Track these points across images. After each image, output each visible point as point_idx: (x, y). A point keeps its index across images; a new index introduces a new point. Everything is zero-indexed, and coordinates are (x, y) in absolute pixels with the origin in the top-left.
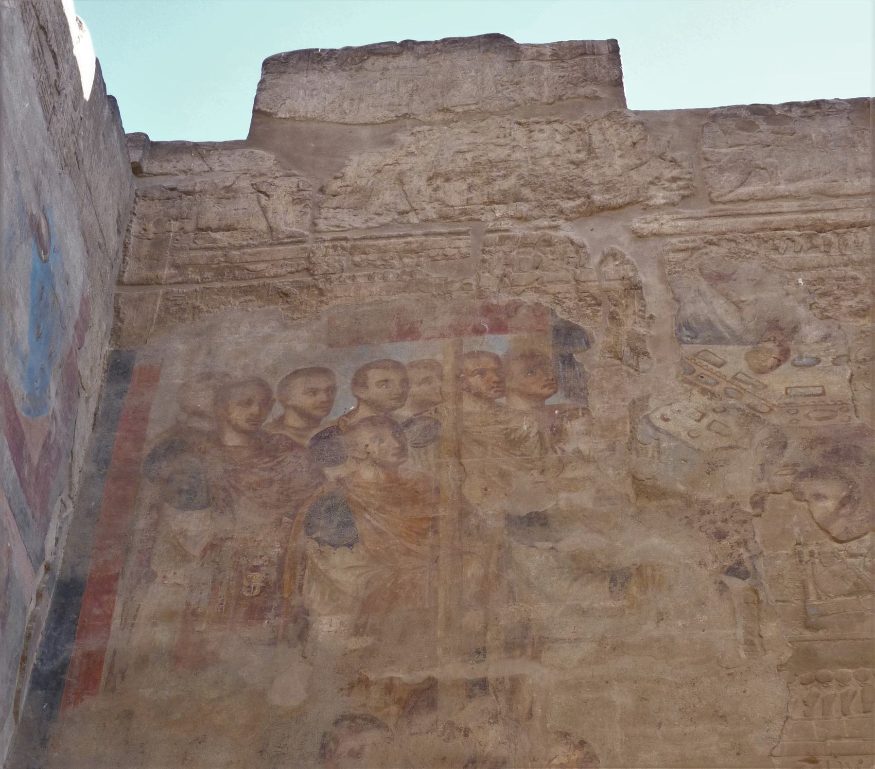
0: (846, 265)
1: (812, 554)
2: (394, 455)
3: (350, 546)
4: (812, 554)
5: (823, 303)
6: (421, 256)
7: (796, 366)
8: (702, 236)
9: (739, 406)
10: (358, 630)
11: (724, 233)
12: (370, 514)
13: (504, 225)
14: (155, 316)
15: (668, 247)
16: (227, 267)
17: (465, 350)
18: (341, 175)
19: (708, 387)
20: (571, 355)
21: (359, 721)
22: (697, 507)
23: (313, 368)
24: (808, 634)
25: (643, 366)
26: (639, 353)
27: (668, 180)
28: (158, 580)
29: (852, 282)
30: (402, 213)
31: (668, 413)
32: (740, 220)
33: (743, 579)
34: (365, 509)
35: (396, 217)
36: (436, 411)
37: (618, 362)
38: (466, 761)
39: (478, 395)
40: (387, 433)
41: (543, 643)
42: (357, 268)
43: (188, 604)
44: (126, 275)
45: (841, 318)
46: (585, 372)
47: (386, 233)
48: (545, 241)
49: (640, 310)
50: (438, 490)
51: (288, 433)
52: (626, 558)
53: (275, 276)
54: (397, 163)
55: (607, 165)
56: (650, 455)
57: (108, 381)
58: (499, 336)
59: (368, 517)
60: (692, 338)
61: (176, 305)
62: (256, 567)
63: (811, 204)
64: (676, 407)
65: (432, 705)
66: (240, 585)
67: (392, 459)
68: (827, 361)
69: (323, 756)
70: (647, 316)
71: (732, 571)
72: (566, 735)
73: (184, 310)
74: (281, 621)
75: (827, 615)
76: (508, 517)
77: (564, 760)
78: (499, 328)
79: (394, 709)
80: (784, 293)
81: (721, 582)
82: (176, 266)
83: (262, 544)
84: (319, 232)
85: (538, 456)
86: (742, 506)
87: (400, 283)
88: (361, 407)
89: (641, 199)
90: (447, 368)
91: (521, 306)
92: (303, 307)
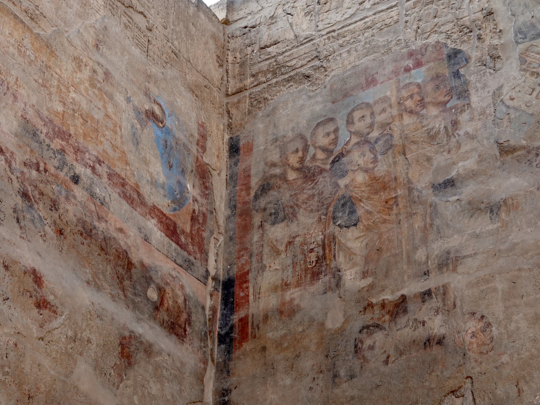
2: (371, 163)
3: (355, 225)
6: (373, 30)
10: (364, 275)
12: (363, 203)
16: (278, 68)
17: (402, 85)
19: (535, 70)
20: (458, 70)
21: (371, 328)
22: (534, 152)
25: (498, 66)
28: (267, 269)
31: (514, 95)
34: (360, 200)
36: (390, 129)
37: (484, 67)
38: (425, 341)
39: (411, 112)
41: (458, 260)
42: (342, 48)
43: (283, 280)
44: (230, 90)
46: (466, 80)
49: (494, 28)
50: (396, 179)
52: (499, 196)
56: (505, 126)
57: (230, 157)
58: (418, 70)
59: (362, 205)
60: (523, 39)
62: (312, 249)
64: (517, 89)
66: (305, 262)
69: (356, 352)
70: (498, 31)
72: (473, 314)
73: (260, 102)
74: (327, 278)
77: (474, 329)
78: (419, 64)
79: (387, 317)
82: (253, 76)
83: (313, 235)
85: (446, 142)
88: (352, 137)
92: (317, 82)
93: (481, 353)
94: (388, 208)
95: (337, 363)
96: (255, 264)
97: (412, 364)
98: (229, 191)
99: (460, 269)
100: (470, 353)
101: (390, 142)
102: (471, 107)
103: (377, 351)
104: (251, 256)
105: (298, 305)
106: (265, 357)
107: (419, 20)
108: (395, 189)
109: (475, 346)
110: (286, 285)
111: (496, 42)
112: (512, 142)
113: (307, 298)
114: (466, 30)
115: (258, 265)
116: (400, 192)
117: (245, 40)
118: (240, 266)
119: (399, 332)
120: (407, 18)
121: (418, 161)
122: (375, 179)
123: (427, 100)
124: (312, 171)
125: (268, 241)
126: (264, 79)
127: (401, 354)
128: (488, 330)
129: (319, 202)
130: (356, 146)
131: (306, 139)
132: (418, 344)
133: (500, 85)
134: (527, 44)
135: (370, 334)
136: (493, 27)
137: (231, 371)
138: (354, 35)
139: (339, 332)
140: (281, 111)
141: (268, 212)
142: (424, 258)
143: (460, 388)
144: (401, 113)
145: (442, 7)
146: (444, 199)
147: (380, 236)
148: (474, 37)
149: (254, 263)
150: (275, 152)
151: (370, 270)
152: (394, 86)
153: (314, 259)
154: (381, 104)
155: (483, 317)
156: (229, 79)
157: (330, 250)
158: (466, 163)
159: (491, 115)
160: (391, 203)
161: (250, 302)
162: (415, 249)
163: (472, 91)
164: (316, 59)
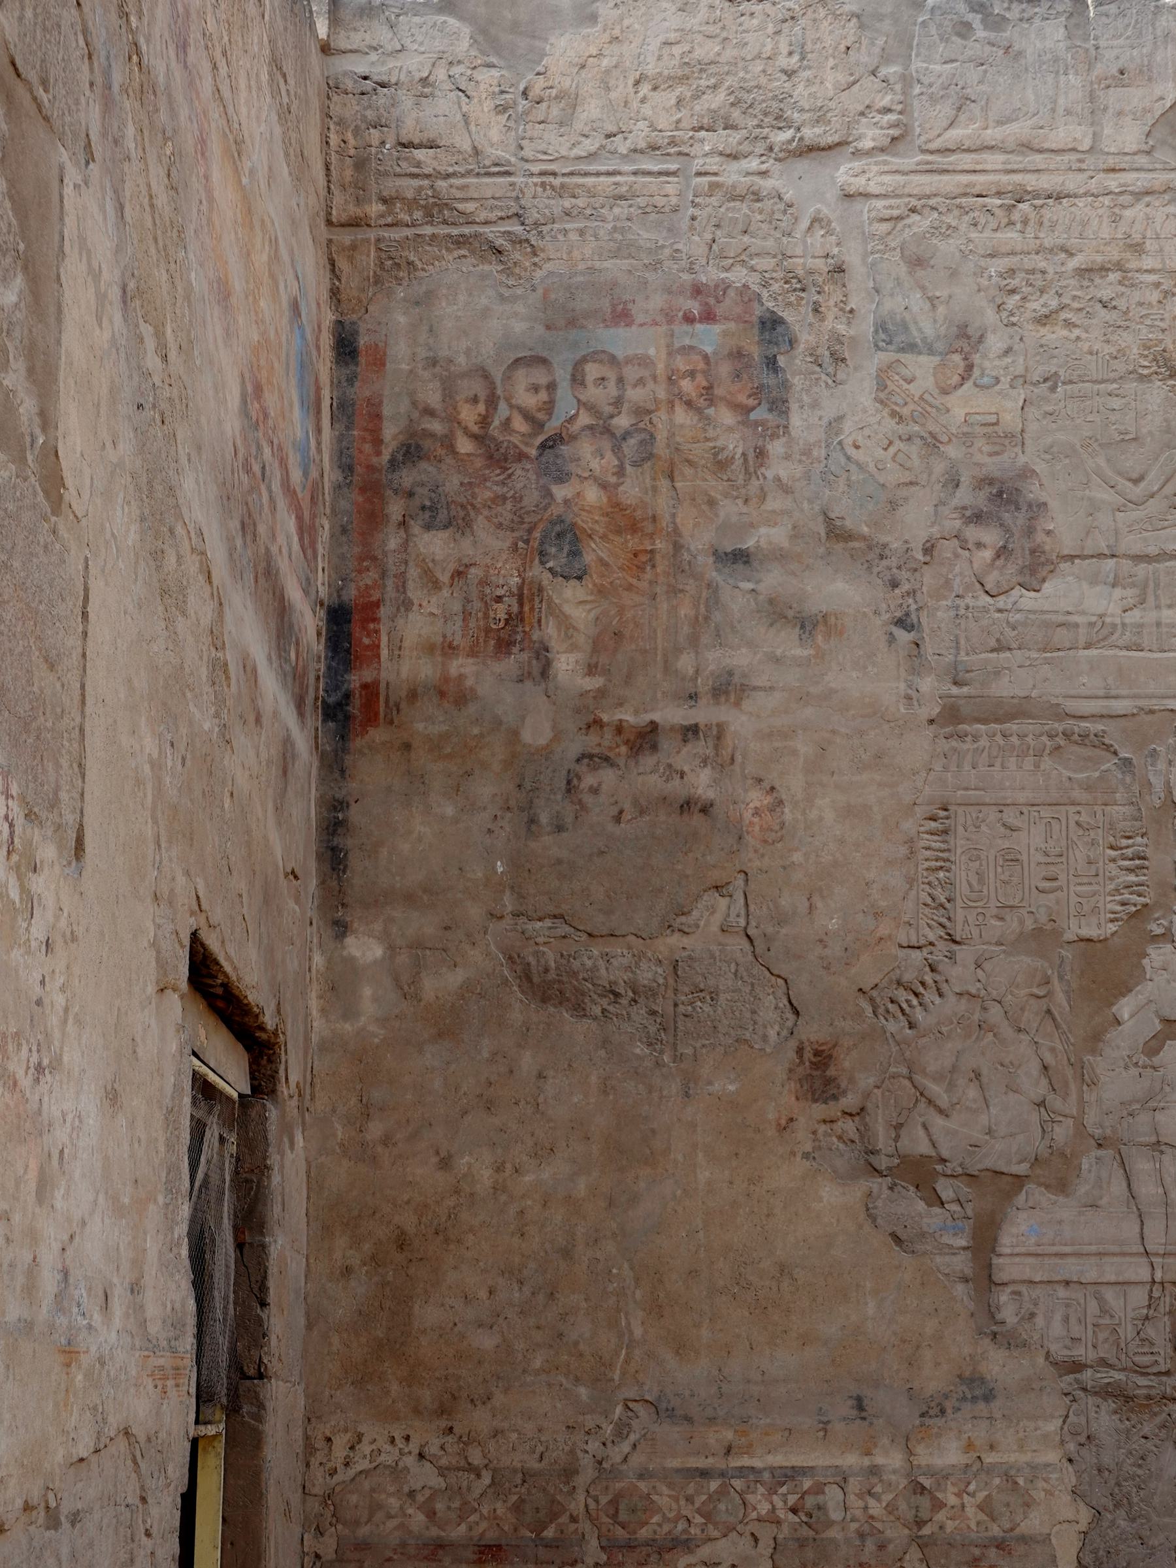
1: (967, 608)
3: (579, 578)
4: (967, 608)
10: (591, 670)
11: (929, 197)
13: (713, 163)
15: (873, 214)
16: (435, 204)
17: (677, 345)
22: (878, 551)
24: (955, 690)
25: (841, 376)
27: (879, 112)
28: (415, 608)
29: (1039, 276)
30: (608, 136)
32: (946, 178)
37: (818, 369)
39: (689, 404)
40: (606, 444)
43: (444, 636)
44: (334, 212)
48: (753, 193)
50: (654, 519)
51: (516, 439)
52: (815, 606)
54: (600, 55)
55: (818, 81)
63: (1016, 161)
64: (867, 432)
65: (654, 747)
67: (613, 480)
68: (1005, 381)
69: (569, 791)
71: (901, 623)
72: (760, 781)
73: (398, 265)
74: (525, 656)
77: (758, 804)
78: (709, 317)
79: (623, 749)
82: (385, 201)
90: (660, 367)
92: (517, 270)
93: (765, 841)
95: (536, 801)
97: (658, 832)
99: (746, 705)
100: (749, 838)
104: (383, 575)
105: (472, 690)
107: (717, 226)
108: (651, 536)
109: (757, 828)
110: (450, 646)
111: (841, 328)
112: (848, 523)
113: (489, 679)
114: (798, 284)
117: (365, 109)
119: (640, 778)
123: (719, 391)
127: (642, 812)
130: (588, 432)
135: (594, 769)
142: (691, 671)
145: (759, 217)
146: (731, 581)
147: (621, 610)
149: (389, 589)
150: (431, 385)
153: (502, 616)
155: (773, 789)
157: (532, 609)
158: (773, 531)
160: (644, 558)
162: (678, 650)
163: (794, 406)
164: (515, 219)
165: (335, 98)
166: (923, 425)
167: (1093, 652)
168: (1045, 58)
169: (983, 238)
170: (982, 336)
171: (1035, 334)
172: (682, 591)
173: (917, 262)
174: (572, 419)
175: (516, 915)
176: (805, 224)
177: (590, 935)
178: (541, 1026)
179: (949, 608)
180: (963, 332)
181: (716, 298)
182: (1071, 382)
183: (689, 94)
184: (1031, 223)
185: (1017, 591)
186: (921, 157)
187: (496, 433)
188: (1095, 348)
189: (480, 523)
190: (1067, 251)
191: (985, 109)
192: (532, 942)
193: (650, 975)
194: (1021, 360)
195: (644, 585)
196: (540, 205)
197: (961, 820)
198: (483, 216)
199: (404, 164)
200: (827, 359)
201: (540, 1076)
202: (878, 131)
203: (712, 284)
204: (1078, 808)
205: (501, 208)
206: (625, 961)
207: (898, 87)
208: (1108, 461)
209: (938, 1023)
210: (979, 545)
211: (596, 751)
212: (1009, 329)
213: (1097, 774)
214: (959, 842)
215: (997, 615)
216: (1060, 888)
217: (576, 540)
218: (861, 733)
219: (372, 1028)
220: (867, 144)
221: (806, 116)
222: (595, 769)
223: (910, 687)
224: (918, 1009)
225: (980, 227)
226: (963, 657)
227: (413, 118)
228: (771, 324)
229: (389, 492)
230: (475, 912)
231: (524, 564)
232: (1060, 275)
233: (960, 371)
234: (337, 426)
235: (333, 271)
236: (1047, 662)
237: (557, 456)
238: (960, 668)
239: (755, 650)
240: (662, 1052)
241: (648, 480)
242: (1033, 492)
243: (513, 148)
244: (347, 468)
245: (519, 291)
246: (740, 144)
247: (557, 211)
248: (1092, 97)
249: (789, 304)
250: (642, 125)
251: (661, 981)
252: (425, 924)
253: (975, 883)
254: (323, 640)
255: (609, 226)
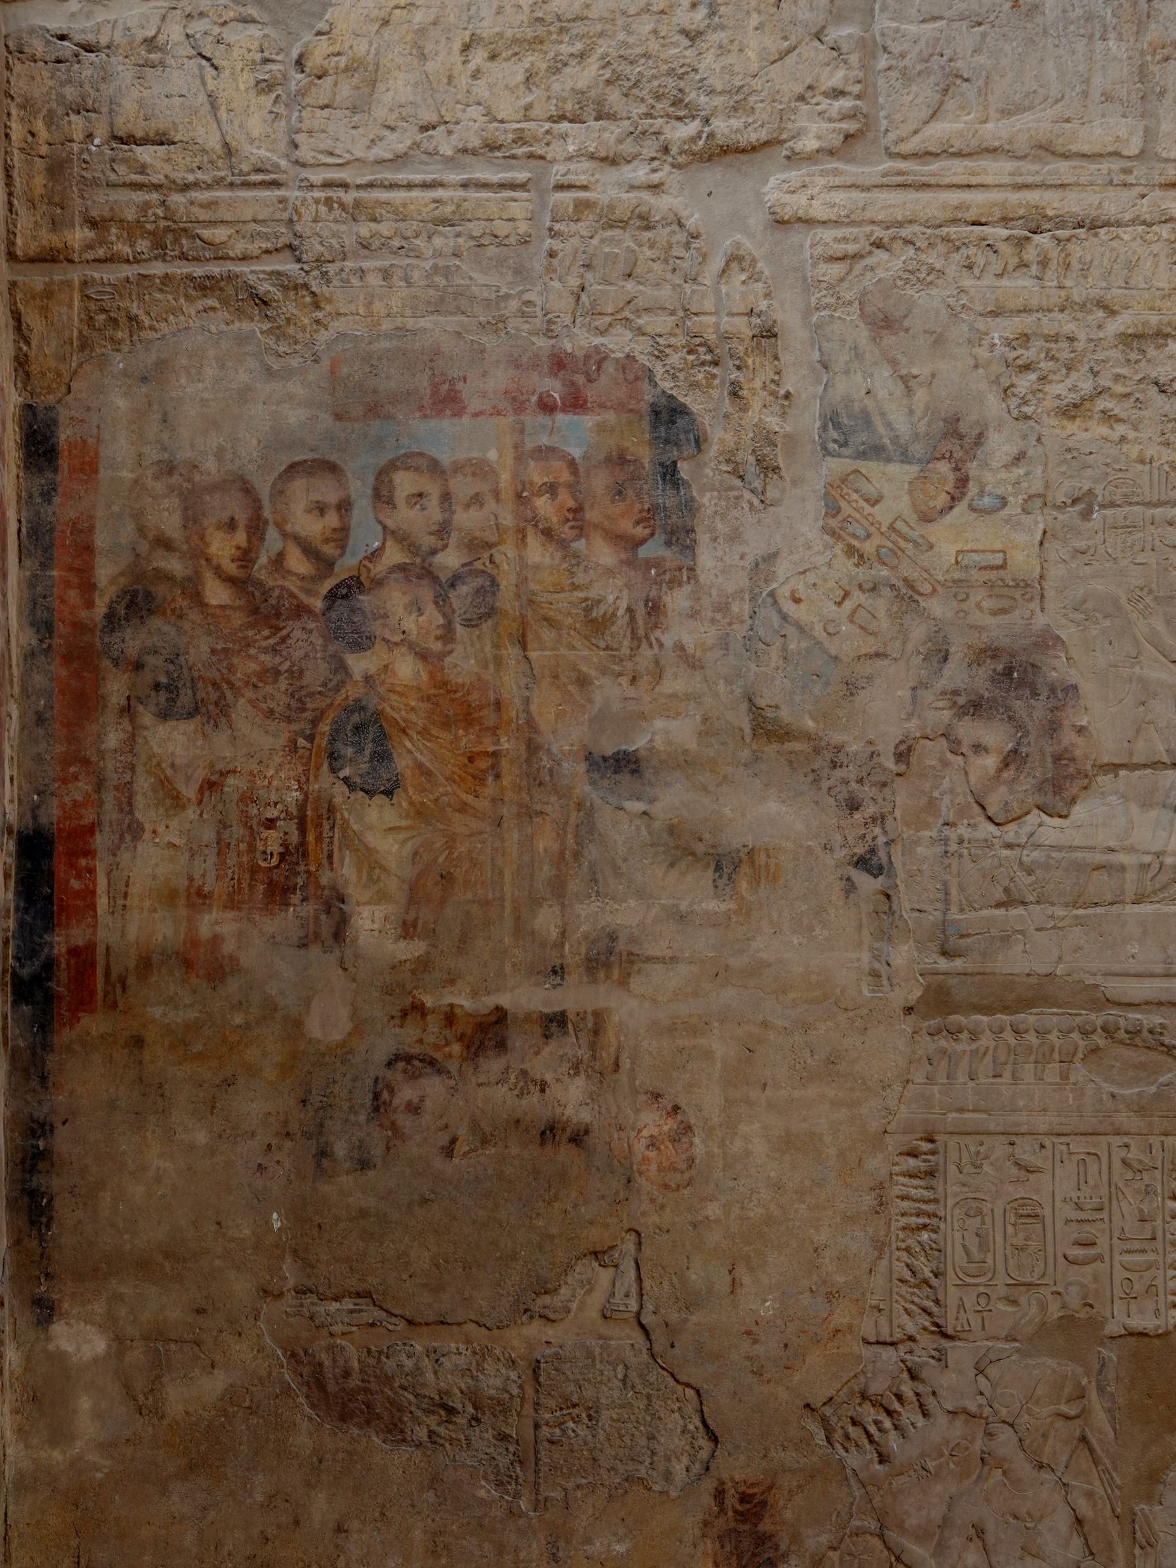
0: (1061, 311)
1: (961, 841)
2: (437, 638)
3: (389, 793)
4: (961, 841)
5: (1025, 382)
6: (458, 235)
7: (974, 510)
8: (868, 229)
9: (894, 581)
10: (408, 930)
11: (900, 225)
13: (581, 171)
14: (75, 334)
15: (819, 250)
16: (168, 229)
17: (529, 445)
18: (326, 28)
19: (856, 543)
20: (675, 463)
21: (416, 1063)
22: (828, 756)
23: (314, 461)
24: (943, 964)
25: (772, 493)
26: (768, 468)
27: (826, 95)
28: (147, 836)
29: (1064, 344)
30: (425, 128)
32: (926, 196)
33: (876, 877)
34: (404, 731)
35: (419, 137)
36: (492, 562)
37: (738, 482)
39: (548, 533)
40: (426, 593)
41: (632, 962)
43: (191, 879)
44: (19, 241)
45: (1045, 419)
46: (693, 499)
47: (402, 177)
48: (641, 217)
49: (773, 381)
50: (498, 705)
51: (292, 585)
52: (735, 837)
53: (245, 258)
55: (735, 47)
56: (773, 665)
57: (27, 468)
59: (409, 745)
60: (841, 446)
61: (103, 310)
63: (1031, 171)
64: (811, 577)
65: (502, 1046)
66: (251, 848)
67: (437, 646)
68: (1016, 502)
69: (376, 1109)
70: (782, 392)
71: (862, 863)
72: (657, 1096)
73: (114, 322)
74: (309, 909)
75: (968, 935)
76: (589, 757)
78: (576, 403)
79: (456, 1048)
80: (972, 362)
81: (848, 879)
82: (93, 224)
83: (275, 783)
84: (304, 165)
86: (882, 759)
87: (431, 292)
88: (388, 544)
89: (784, 136)
90: (505, 477)
91: (605, 358)
92: (291, 330)
93: (666, 1186)
94: (474, 777)
95: (329, 1123)
96: (110, 812)
98: (28, 573)
99: (635, 983)
100: (641, 1181)
101: (489, 599)
102: (697, 581)
103: (426, 1119)
104: (99, 786)
105: (231, 957)
106: (141, 1062)
108: (494, 731)
109: (654, 1167)
110: (199, 893)
111: (772, 421)
112: (785, 714)
113: (258, 942)
114: (709, 354)
115: (120, 816)
116: (506, 746)
117: (62, 85)
118: (69, 805)
119: (481, 1091)
120: (556, 244)
121: (556, 677)
122: (443, 686)
123: (592, 515)
124: (273, 601)
125: (150, 758)
126: (127, 250)
127: (485, 1142)
128: (684, 1139)
129: (292, 695)
130: (399, 575)
131: (259, 500)
132: (527, 1130)
133: (773, 550)
134: (847, 465)
136: (772, 376)
137: (51, 1079)
138: (402, 225)
139: (339, 1052)
140: (183, 381)
141: (147, 677)
142: (554, 933)
143: (612, 1248)
144: (522, 525)
147: (451, 842)
148: (723, 382)
150: (166, 503)
151: (420, 922)
152: (508, 440)
153: (275, 848)
154: (469, 478)
156: (16, 202)
157: (319, 838)
158: (674, 725)
159: (742, 622)
160: (483, 764)
161: (99, 912)
162: (536, 902)
163: (703, 538)
165: (18, 68)
166: (894, 568)
167: (1147, 908)
168: (1072, 15)
169: (982, 288)
170: (981, 435)
171: (1057, 431)
172: (540, 813)
173: (884, 324)
174: (374, 556)
175: (301, 1291)
176: (717, 263)
177: (410, 1322)
178: (341, 1456)
179: (933, 841)
180: (952, 428)
181: (587, 374)
182: (1113, 505)
183: (544, 66)
184: (1053, 265)
185: (1034, 817)
186: (889, 164)
187: (262, 576)
188: (1149, 453)
189: (241, 709)
190: (1105, 308)
191: (983, 93)
192: (325, 1332)
193: (498, 1382)
194: (1039, 471)
195: (483, 804)
196: (324, 231)
197: (953, 1156)
198: (239, 247)
199: (122, 169)
200: (752, 469)
201: (340, 1529)
202: (825, 125)
203: (580, 354)
204: (1126, 1140)
205: (266, 237)
206: (462, 1361)
207: (854, 58)
208: (1168, 622)
209: (922, 1455)
210: (978, 748)
211: (416, 1050)
212: (1021, 425)
213: (1153, 1089)
214: (951, 1188)
215: (1005, 853)
216: (1099, 1258)
217: (383, 736)
218: (806, 1028)
219: (93, 1457)
220: (809, 144)
221: (718, 101)
222: (414, 1077)
223: (877, 958)
224: (893, 1434)
225: (977, 271)
226: (954, 915)
227: (133, 99)
228: (668, 416)
229: (106, 663)
230: (241, 1287)
231: (306, 772)
232: (1096, 343)
233: (949, 487)
234: (28, 562)
235: (18, 328)
236: (1079, 922)
237: (353, 611)
238: (951, 931)
239: (645, 902)
240: (517, 1495)
241: (488, 649)
242: (1057, 669)
243: (283, 145)
244: (44, 627)
245: (295, 362)
246: (620, 141)
247: (349, 242)
248: (1143, 74)
249: (694, 385)
250: (475, 112)
251: (515, 1391)
252: (167, 1306)
253: (974, 1249)
254: (12, 884)
255: (427, 265)
